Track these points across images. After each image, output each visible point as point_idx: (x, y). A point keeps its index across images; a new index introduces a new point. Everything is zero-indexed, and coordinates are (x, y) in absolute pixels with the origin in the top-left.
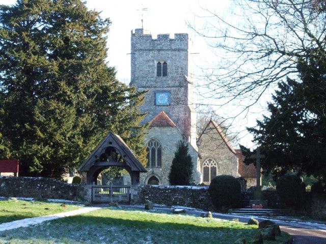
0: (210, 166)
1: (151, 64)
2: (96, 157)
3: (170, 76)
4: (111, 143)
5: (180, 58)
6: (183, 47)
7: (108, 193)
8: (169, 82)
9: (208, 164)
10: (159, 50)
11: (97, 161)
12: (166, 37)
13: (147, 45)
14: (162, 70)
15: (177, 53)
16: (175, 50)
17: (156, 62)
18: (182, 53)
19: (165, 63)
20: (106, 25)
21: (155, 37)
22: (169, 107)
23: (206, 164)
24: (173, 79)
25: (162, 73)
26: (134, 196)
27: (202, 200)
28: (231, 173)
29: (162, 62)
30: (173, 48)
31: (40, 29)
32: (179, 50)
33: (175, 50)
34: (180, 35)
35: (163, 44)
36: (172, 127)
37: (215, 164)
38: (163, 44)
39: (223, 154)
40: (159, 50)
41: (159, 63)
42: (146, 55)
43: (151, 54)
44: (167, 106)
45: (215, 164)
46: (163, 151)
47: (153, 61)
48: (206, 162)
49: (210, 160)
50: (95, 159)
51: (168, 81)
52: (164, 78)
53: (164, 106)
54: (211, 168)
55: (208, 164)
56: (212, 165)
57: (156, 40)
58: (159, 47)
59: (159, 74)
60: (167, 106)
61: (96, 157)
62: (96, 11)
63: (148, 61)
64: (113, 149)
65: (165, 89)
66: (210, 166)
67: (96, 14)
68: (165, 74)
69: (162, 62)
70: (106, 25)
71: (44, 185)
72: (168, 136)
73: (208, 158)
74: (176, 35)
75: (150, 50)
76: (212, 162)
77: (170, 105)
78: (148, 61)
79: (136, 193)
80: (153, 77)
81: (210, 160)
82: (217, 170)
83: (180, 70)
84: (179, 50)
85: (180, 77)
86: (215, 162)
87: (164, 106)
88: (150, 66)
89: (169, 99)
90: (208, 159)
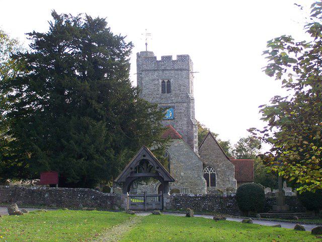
0: (210, 173)
1: (157, 82)
2: (131, 169)
3: (174, 92)
4: (144, 156)
5: (182, 77)
6: (184, 67)
7: (143, 201)
10: (163, 70)
11: (132, 173)
12: (169, 58)
13: (153, 66)
14: (166, 87)
15: (179, 72)
16: (177, 70)
17: (161, 81)
18: (184, 73)
19: (169, 81)
20: (129, 48)
21: (159, 59)
24: (176, 96)
25: (166, 90)
26: (167, 203)
27: (229, 206)
29: (166, 81)
31: (70, 53)
32: (181, 70)
33: (177, 70)
34: (181, 56)
35: (167, 64)
36: (179, 138)
37: (214, 171)
38: (167, 64)
39: (221, 162)
40: (163, 70)
41: (163, 82)
43: (156, 73)
45: (214, 171)
46: (171, 160)
47: (158, 79)
49: (210, 168)
50: (130, 171)
51: (172, 97)
52: (169, 95)
55: (208, 171)
56: (211, 171)
57: (160, 61)
58: (163, 67)
59: (163, 92)
61: (131, 169)
62: (121, 36)
64: (147, 162)
65: (169, 105)
66: (210, 173)
67: (122, 38)
68: (169, 91)
69: (166, 81)
70: (129, 48)
71: (84, 195)
72: (175, 147)
74: (178, 56)
75: (155, 70)
78: (154, 80)
79: (169, 201)
80: (157, 94)
81: (210, 168)
83: (182, 87)
84: (181, 70)
88: (155, 84)
89: (174, 114)
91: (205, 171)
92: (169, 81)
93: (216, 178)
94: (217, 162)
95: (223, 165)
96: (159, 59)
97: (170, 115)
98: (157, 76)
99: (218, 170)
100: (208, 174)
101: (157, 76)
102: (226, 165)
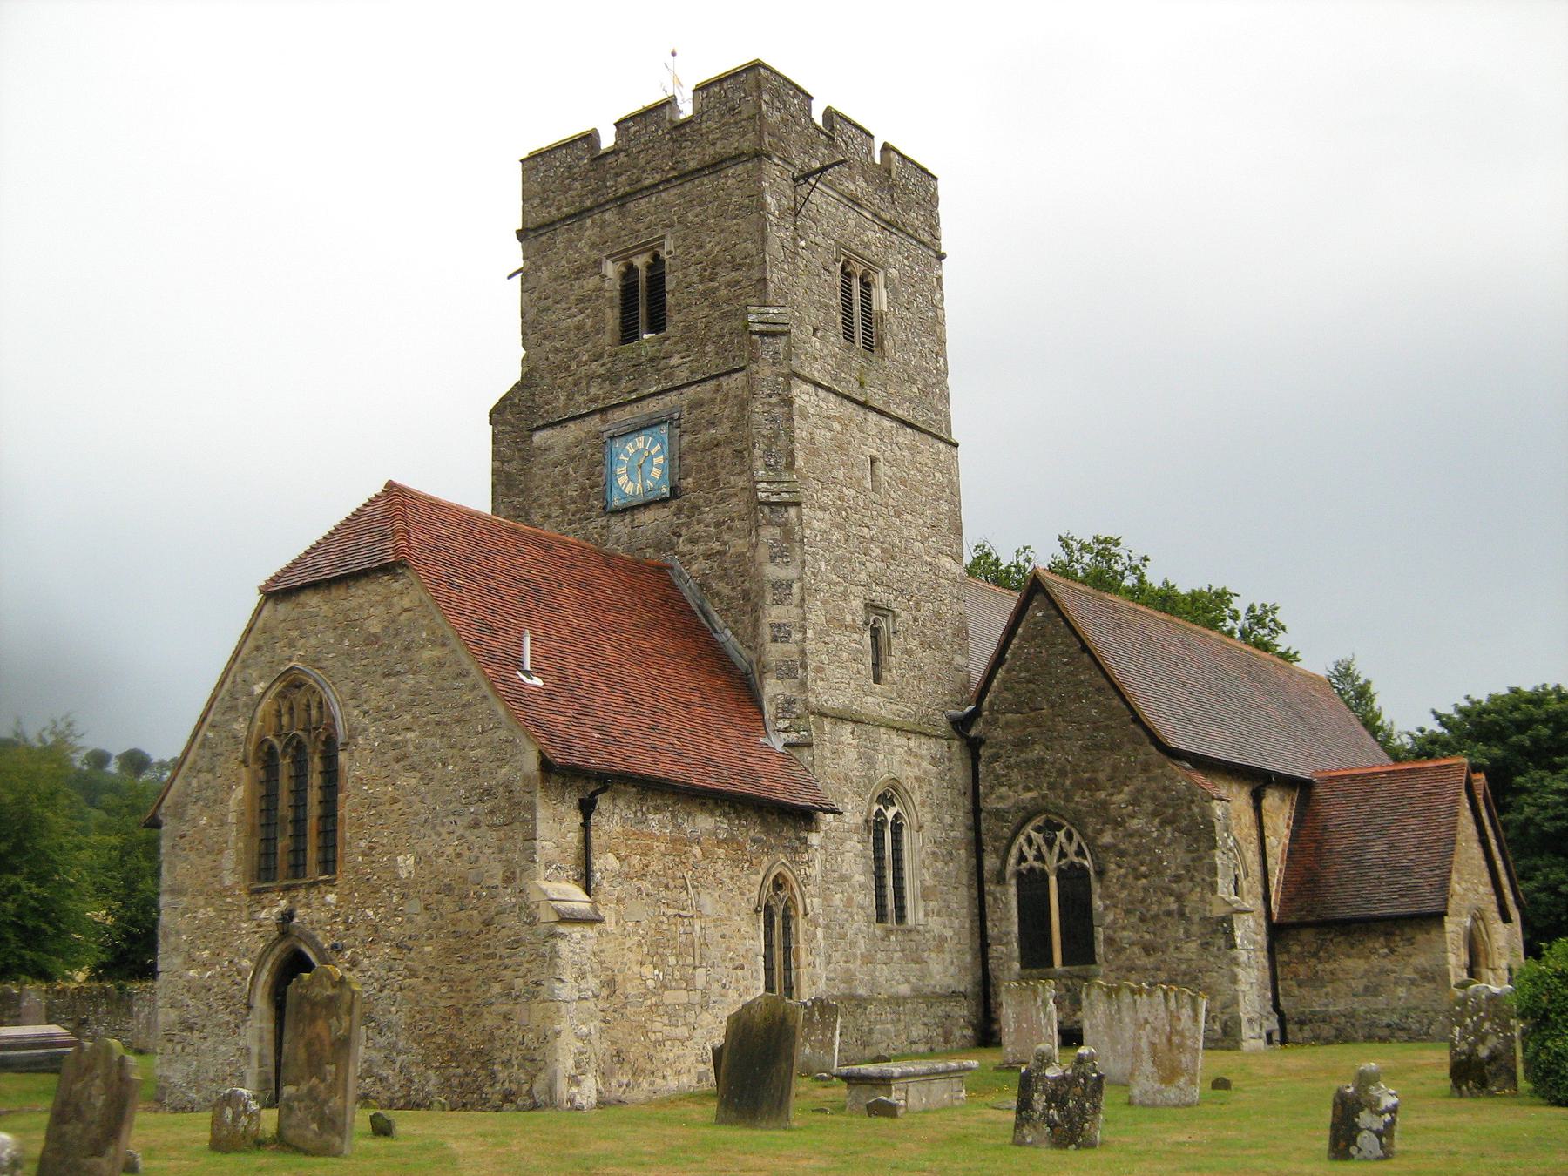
3: (675, 322)
8: (675, 361)
9: (1039, 857)
10: (622, 201)
15: (707, 183)
17: (611, 269)
22: (675, 503)
23: (1030, 854)
28: (1180, 898)
30: (693, 165)
34: (720, 81)
39: (1118, 779)
41: (630, 270)
42: (570, 244)
43: (590, 229)
44: (663, 501)
45: (1080, 853)
47: (598, 264)
48: (1030, 841)
49: (1050, 828)
51: (668, 357)
53: (646, 505)
54: (1060, 873)
56: (1063, 855)
60: (663, 501)
63: (579, 272)
66: (1052, 863)
68: (657, 324)
69: (640, 262)
73: (1037, 813)
75: (581, 214)
76: (1061, 835)
77: (675, 492)
81: (1050, 828)
82: (1096, 888)
85: (724, 316)
86: (1076, 836)
87: (646, 505)
89: (677, 462)
90: (1039, 821)
91: (1022, 858)
92: (656, 257)
93: (1098, 903)
94: (1093, 785)
95: (1135, 801)
96: (608, 140)
97: (656, 473)
98: (593, 246)
99: (1107, 839)
100: (1044, 877)
101: (593, 246)
102: (1154, 798)
